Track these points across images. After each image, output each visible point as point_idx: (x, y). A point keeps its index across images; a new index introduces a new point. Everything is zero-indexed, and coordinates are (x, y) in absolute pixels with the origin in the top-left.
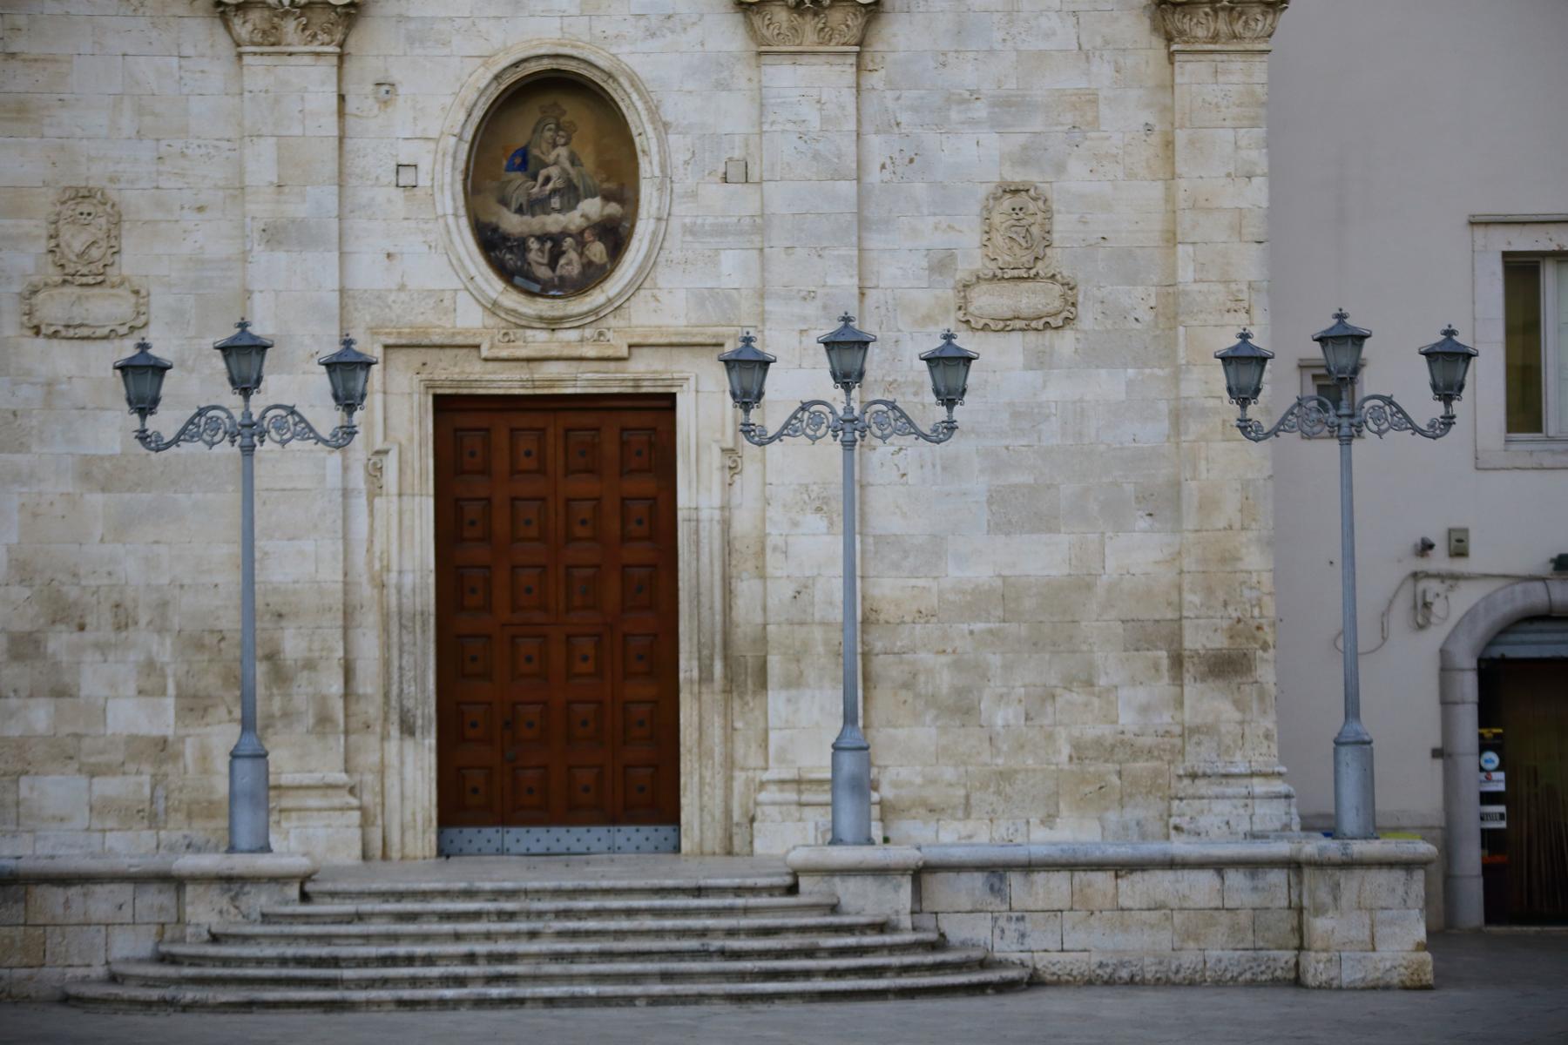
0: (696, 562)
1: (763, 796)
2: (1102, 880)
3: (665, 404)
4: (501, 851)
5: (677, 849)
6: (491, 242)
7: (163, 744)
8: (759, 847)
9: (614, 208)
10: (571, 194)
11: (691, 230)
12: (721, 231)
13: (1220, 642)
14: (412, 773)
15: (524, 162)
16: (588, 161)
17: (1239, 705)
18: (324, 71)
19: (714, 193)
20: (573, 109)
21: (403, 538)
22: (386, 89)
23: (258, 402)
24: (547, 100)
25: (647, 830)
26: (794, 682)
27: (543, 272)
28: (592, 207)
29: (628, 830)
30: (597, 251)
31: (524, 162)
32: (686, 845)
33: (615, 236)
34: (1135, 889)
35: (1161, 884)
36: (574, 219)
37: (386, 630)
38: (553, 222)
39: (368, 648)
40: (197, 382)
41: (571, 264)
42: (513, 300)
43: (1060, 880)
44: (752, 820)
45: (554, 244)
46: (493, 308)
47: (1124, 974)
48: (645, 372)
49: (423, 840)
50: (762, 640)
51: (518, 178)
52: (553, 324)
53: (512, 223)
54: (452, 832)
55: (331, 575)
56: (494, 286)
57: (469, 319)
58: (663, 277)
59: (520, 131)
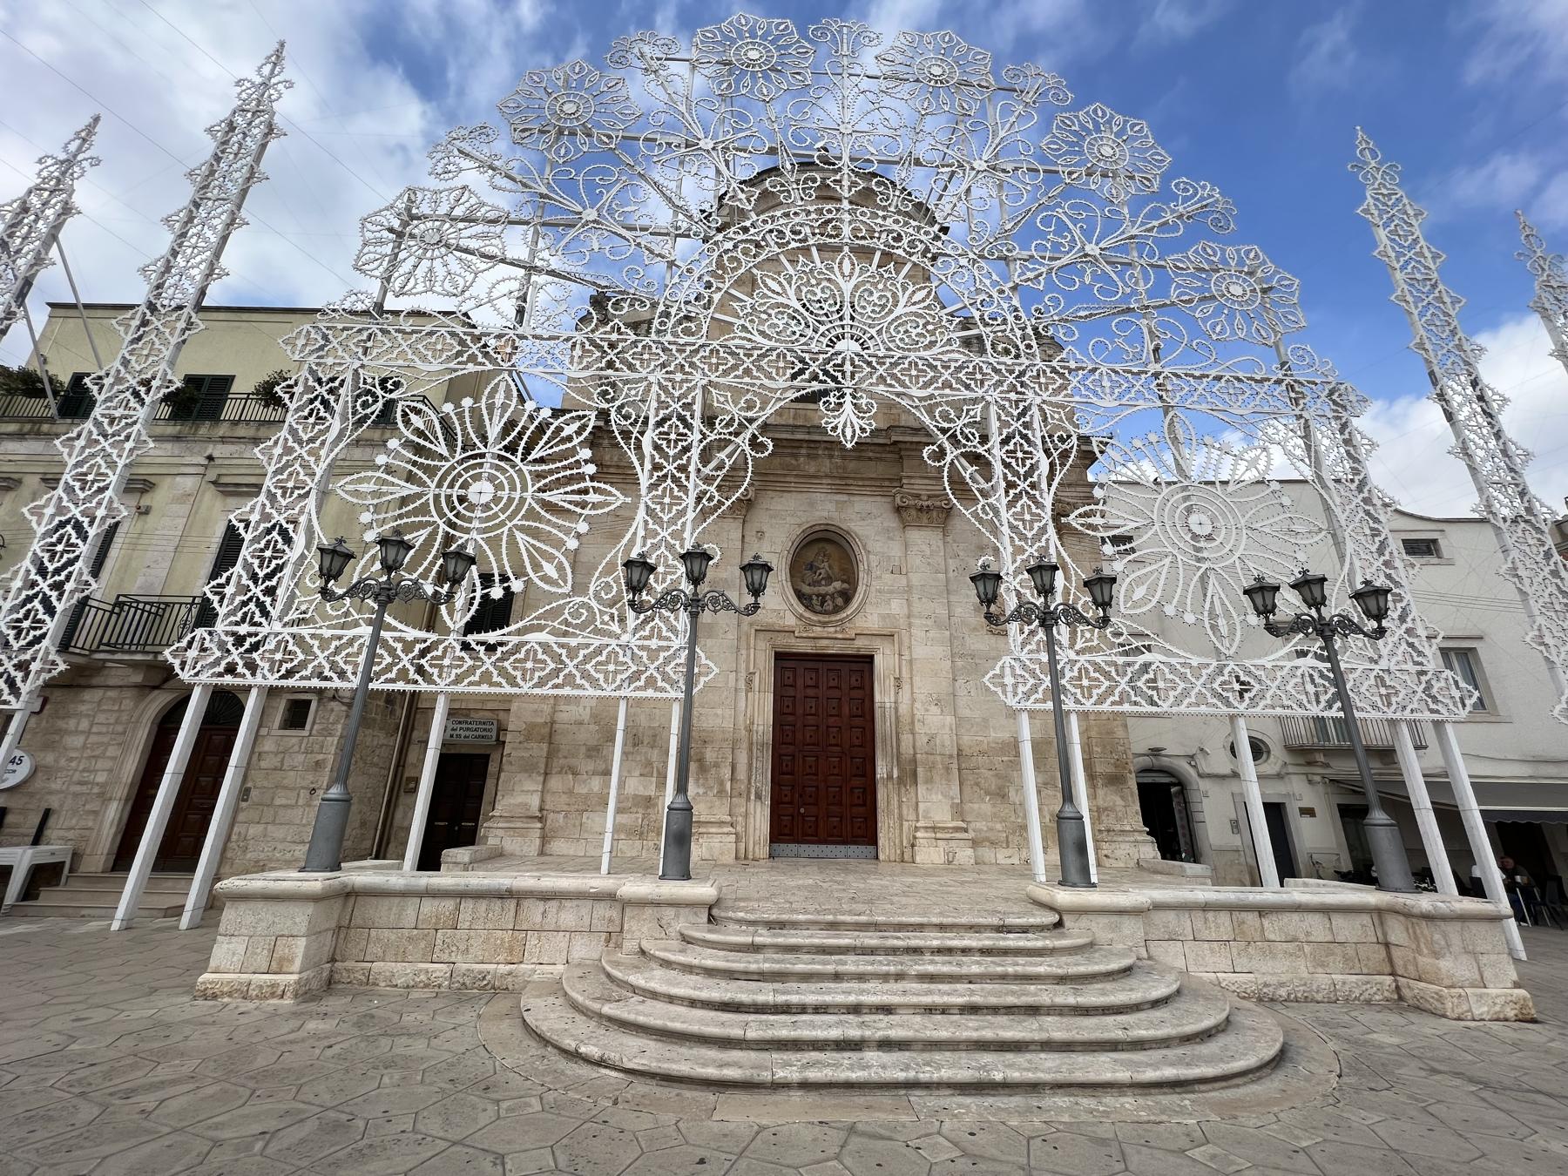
0: (883, 726)
1: (919, 834)
2: (1251, 918)
3: (869, 659)
4: (797, 856)
5: (877, 858)
6: (800, 596)
7: (649, 799)
8: (918, 859)
9: (846, 586)
10: (829, 580)
11: (879, 591)
12: (892, 592)
13: (1110, 770)
14: (760, 818)
15: (811, 567)
16: (836, 570)
17: (1122, 798)
18: (738, 524)
19: (887, 577)
20: (829, 548)
21: (760, 710)
22: (761, 534)
23: (703, 588)
24: (821, 545)
25: (862, 848)
26: (929, 781)
27: (818, 608)
28: (837, 585)
29: (853, 847)
30: (839, 601)
31: (811, 567)
32: (881, 857)
33: (847, 597)
34: (1273, 927)
35: (1293, 922)
36: (830, 589)
37: (751, 750)
38: (823, 590)
39: (742, 758)
40: (671, 576)
41: (829, 606)
42: (808, 614)
43: (1224, 917)
44: (913, 846)
45: (823, 598)
46: (800, 617)
47: (1283, 992)
48: (861, 645)
49: (763, 850)
50: (914, 761)
51: (809, 573)
52: (824, 624)
53: (806, 589)
54: (775, 845)
55: (728, 725)
56: (801, 609)
57: (791, 621)
58: (868, 608)
59: (810, 555)
